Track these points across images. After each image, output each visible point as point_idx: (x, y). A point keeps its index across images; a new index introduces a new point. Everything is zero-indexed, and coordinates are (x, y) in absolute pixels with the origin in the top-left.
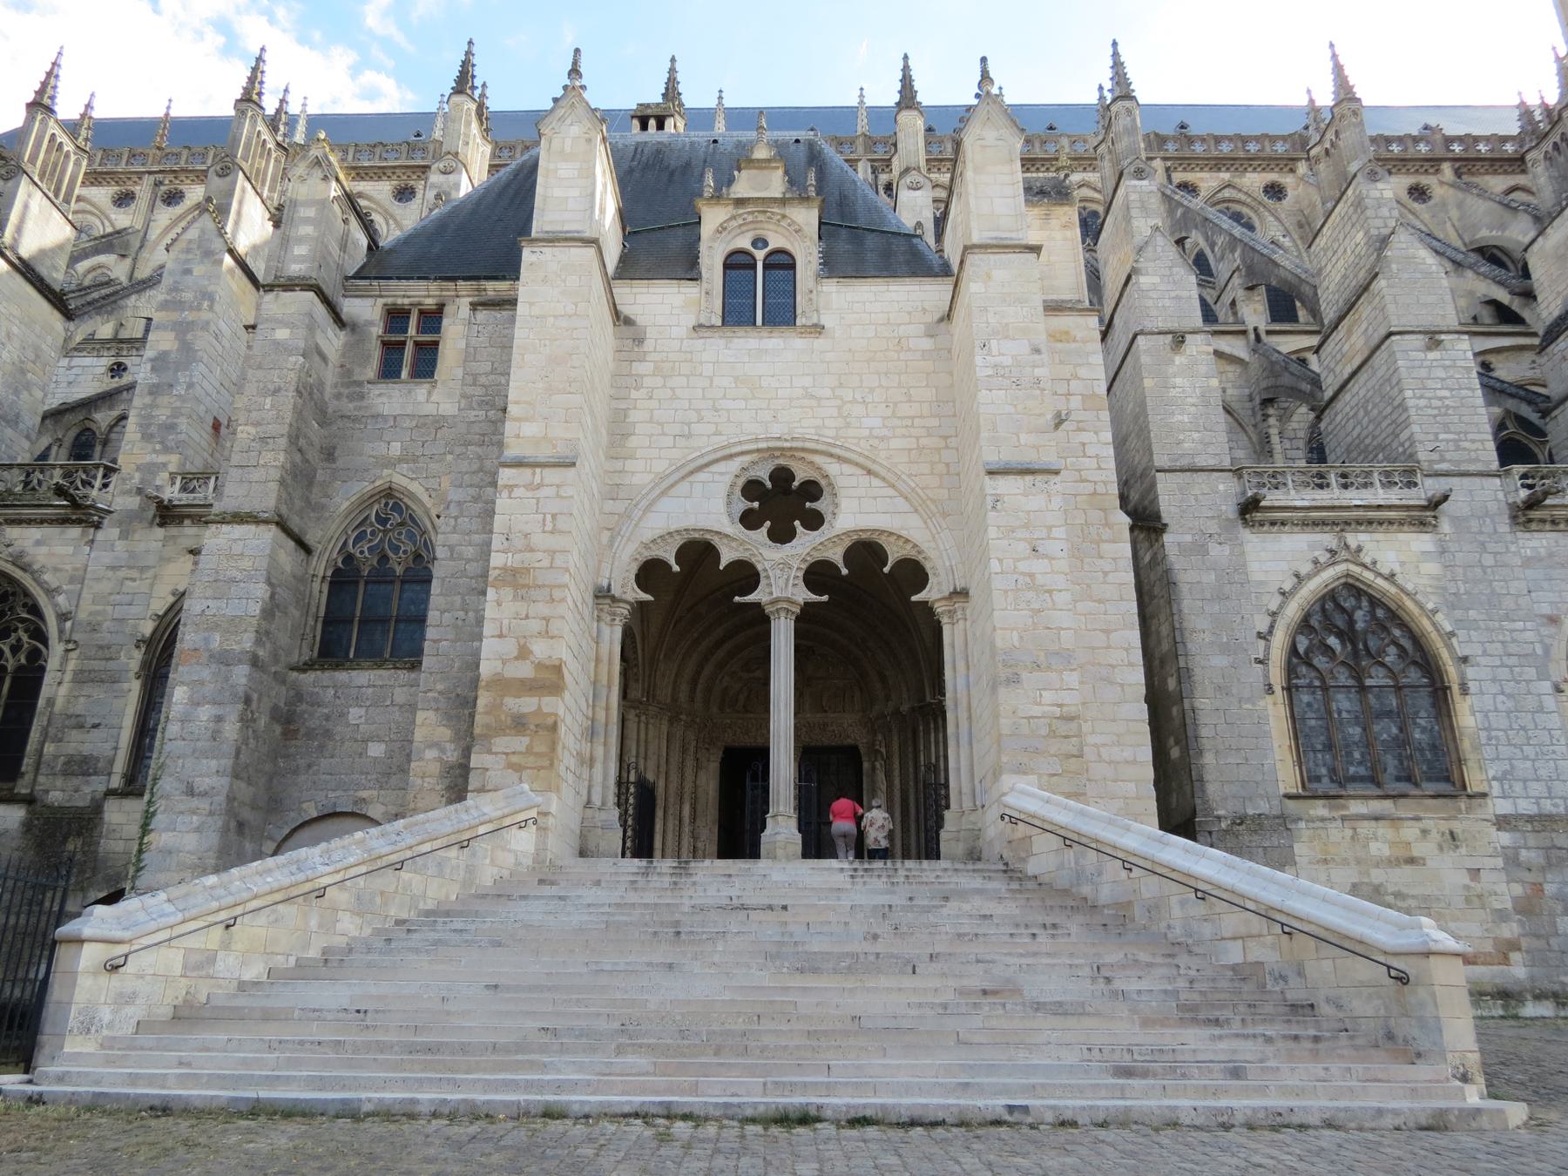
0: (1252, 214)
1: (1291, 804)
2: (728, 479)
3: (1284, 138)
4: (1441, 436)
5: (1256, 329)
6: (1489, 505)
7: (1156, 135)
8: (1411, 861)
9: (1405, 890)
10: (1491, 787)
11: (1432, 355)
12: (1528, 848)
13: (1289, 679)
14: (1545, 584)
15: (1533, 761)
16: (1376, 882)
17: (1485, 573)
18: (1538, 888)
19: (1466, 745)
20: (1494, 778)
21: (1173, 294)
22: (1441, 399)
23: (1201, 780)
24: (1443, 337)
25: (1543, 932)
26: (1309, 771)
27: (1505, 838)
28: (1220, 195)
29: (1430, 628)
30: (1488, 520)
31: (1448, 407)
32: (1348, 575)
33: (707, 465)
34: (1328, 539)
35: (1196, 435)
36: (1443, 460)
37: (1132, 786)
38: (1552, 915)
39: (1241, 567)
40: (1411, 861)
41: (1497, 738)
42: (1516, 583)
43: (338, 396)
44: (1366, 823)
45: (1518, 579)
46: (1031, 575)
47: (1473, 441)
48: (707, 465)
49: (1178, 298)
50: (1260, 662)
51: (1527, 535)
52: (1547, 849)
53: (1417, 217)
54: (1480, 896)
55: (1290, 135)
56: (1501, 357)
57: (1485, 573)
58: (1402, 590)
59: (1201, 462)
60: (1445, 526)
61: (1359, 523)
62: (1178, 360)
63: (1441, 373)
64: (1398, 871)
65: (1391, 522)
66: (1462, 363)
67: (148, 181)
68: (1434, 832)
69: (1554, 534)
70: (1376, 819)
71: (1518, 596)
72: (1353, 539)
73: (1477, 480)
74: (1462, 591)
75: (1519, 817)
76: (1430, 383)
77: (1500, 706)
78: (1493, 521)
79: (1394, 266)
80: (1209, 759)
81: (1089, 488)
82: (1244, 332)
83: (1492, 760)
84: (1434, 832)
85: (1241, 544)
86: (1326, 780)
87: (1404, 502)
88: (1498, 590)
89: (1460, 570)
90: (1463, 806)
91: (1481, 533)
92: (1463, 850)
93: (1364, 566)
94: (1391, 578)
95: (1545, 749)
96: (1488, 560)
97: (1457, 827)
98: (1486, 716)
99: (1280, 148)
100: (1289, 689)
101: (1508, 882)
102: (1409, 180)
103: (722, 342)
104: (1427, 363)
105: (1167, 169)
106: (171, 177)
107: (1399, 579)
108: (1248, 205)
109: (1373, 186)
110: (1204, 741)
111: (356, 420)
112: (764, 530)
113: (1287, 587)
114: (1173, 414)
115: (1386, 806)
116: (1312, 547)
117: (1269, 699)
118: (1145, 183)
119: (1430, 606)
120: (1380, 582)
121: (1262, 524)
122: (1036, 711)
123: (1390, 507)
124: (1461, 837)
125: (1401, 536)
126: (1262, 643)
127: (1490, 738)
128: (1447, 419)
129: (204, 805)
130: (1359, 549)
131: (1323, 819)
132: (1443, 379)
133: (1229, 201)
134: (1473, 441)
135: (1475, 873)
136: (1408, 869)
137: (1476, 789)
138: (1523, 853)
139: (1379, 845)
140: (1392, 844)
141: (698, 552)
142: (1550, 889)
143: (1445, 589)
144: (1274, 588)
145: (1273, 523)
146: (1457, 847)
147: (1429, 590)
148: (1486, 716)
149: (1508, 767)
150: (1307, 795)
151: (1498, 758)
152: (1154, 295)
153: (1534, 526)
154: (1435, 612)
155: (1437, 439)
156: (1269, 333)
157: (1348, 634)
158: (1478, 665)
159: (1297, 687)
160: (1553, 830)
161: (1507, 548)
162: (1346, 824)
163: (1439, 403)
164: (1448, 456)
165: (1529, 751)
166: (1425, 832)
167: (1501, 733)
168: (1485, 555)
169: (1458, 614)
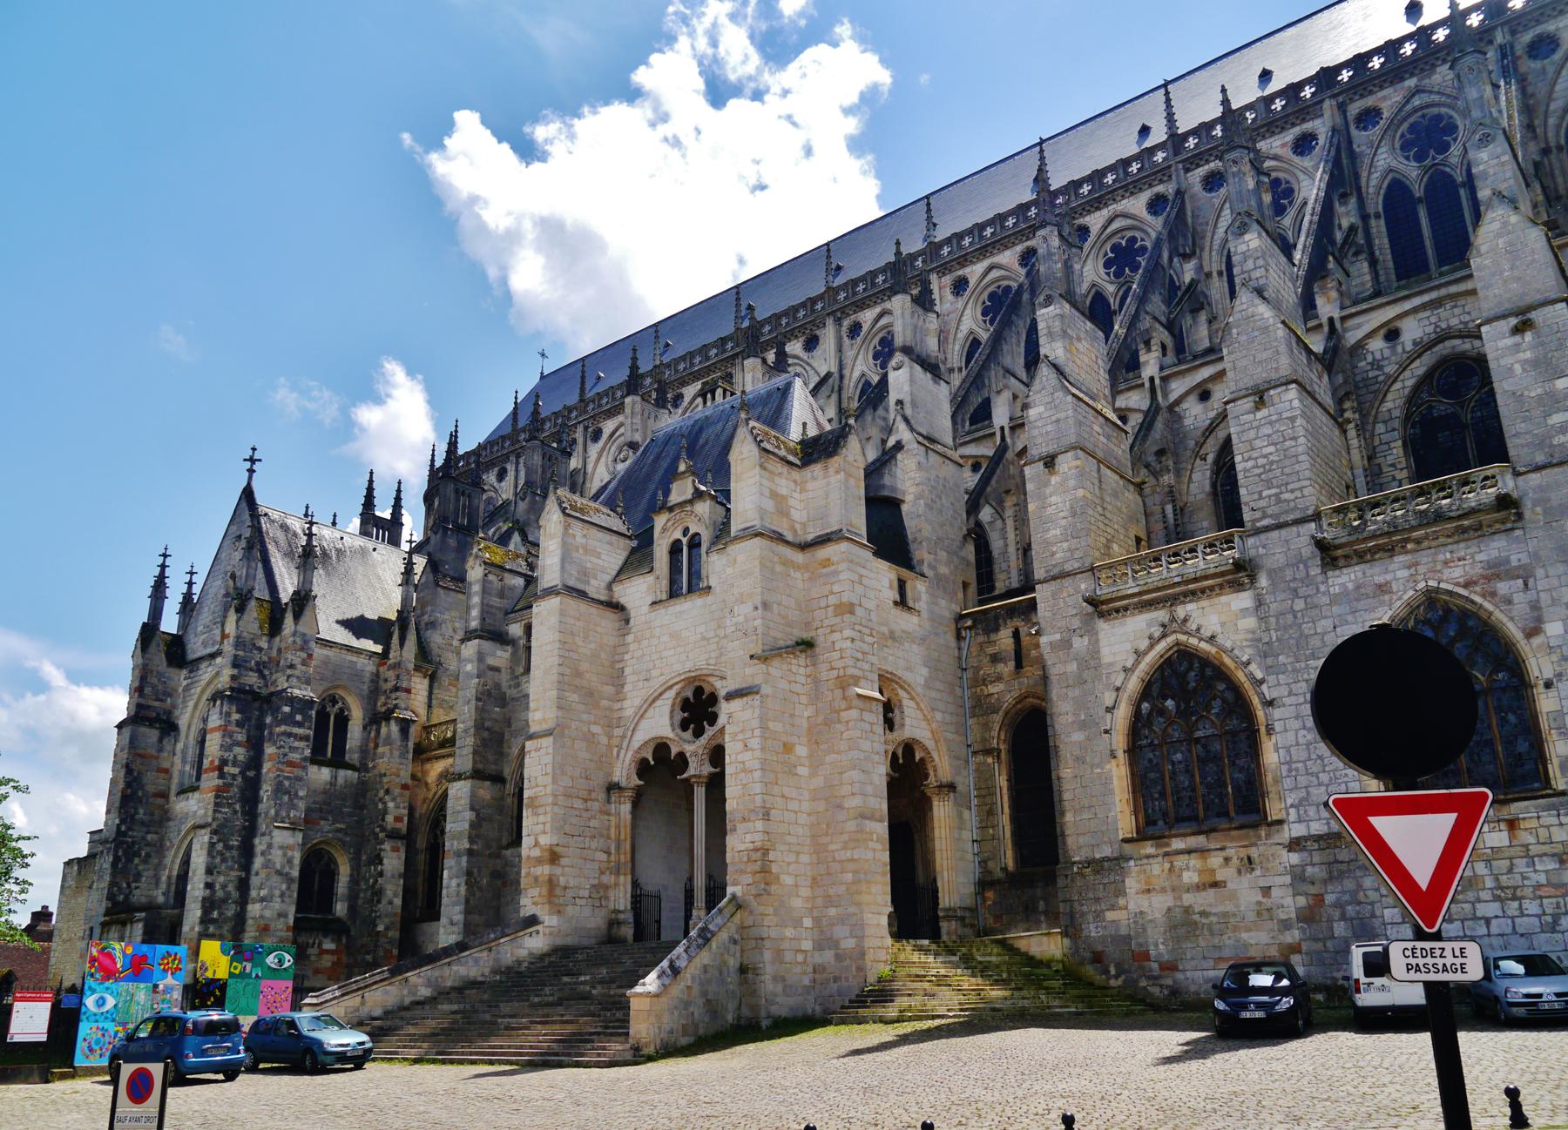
1: (1126, 846)
2: (670, 702)
4: (1264, 494)
5: (1331, 320)
6: (1303, 550)
8: (1215, 885)
9: (1208, 909)
10: (1288, 814)
11: (1259, 415)
12: (1313, 865)
13: (1134, 742)
14: (1350, 618)
15: (1327, 786)
16: (1186, 904)
17: (1295, 617)
18: (1319, 899)
19: (1269, 779)
20: (1292, 806)
21: (1054, 418)
22: (1265, 456)
23: (1063, 834)
24: (1272, 392)
25: (1321, 936)
26: (1147, 816)
27: (1295, 858)
28: (1409, 107)
29: (1243, 678)
30: (1301, 566)
31: (1272, 463)
32: (1178, 643)
33: (660, 695)
34: (1161, 615)
35: (1065, 545)
36: (1264, 516)
37: (850, 875)
38: (1330, 920)
39: (1095, 652)
40: (1215, 885)
41: (1297, 770)
42: (1323, 622)
43: (510, 687)
44: (1181, 857)
45: (1326, 617)
46: (743, 763)
47: (1292, 491)
48: (660, 695)
49: (1058, 421)
50: (1106, 732)
51: (1337, 572)
52: (1330, 864)
54: (1269, 910)
57: (1295, 617)
58: (1222, 649)
59: (1068, 567)
60: (1263, 581)
61: (1185, 595)
62: (1054, 480)
63: (1267, 430)
64: (1203, 894)
65: (1212, 588)
66: (1285, 415)
67: (580, 429)
68: (1235, 858)
69: (1363, 566)
70: (1189, 852)
71: (1324, 634)
72: (1181, 611)
73: (1294, 529)
74: (1274, 639)
75: (1306, 838)
76: (1258, 443)
77: (1301, 740)
78: (1306, 567)
79: (1234, 331)
80: (1069, 817)
81: (835, 673)
82: (1320, 326)
83: (1291, 790)
84: (1235, 858)
85: (1097, 634)
86: (1160, 823)
87: (1218, 570)
88: (1306, 632)
89: (1273, 620)
90: (1263, 833)
91: (1295, 579)
92: (1258, 872)
93: (1188, 634)
94: (1212, 639)
95: (1338, 773)
96: (1299, 605)
97: (1254, 853)
98: (1288, 751)
100: (1133, 751)
101: (1294, 896)
103: (663, 611)
104: (1255, 424)
105: (1342, 108)
106: (591, 421)
107: (1220, 639)
108: (1444, 105)
109: (1241, 240)
110: (1066, 804)
111: (517, 700)
112: (690, 731)
113: (1129, 664)
114: (1049, 530)
115: (1200, 841)
116: (1149, 625)
117: (1114, 762)
118: (1051, 308)
119: (1245, 659)
120: (1203, 645)
121: (1109, 613)
122: (742, 847)
123: (1206, 578)
124: (1257, 861)
125: (1224, 599)
126: (1109, 715)
127: (1290, 770)
128: (1271, 475)
129: (455, 929)
130: (1185, 620)
131: (1148, 857)
132: (1269, 436)
133: (1422, 108)
134: (1292, 491)
135: (1266, 891)
136: (1212, 891)
137: (1275, 818)
138: (1309, 869)
139: (1190, 874)
140: (1200, 872)
141: (661, 748)
142: (1330, 898)
143: (1260, 640)
144: (1119, 667)
145: (1117, 611)
146: (1253, 869)
147: (1245, 644)
148: (1288, 751)
149: (1304, 794)
150: (1141, 836)
151: (1296, 788)
152: (1039, 424)
153: (1342, 562)
154: (1248, 663)
155: (1261, 498)
156: (1343, 319)
157: (1182, 695)
158: (1284, 705)
159: (1141, 747)
160: (1336, 847)
161: (1318, 589)
162: (1166, 858)
163: (1264, 461)
164: (1269, 511)
165: (1324, 777)
166: (1227, 860)
167: (1300, 765)
168: (1296, 601)
169: (1269, 661)
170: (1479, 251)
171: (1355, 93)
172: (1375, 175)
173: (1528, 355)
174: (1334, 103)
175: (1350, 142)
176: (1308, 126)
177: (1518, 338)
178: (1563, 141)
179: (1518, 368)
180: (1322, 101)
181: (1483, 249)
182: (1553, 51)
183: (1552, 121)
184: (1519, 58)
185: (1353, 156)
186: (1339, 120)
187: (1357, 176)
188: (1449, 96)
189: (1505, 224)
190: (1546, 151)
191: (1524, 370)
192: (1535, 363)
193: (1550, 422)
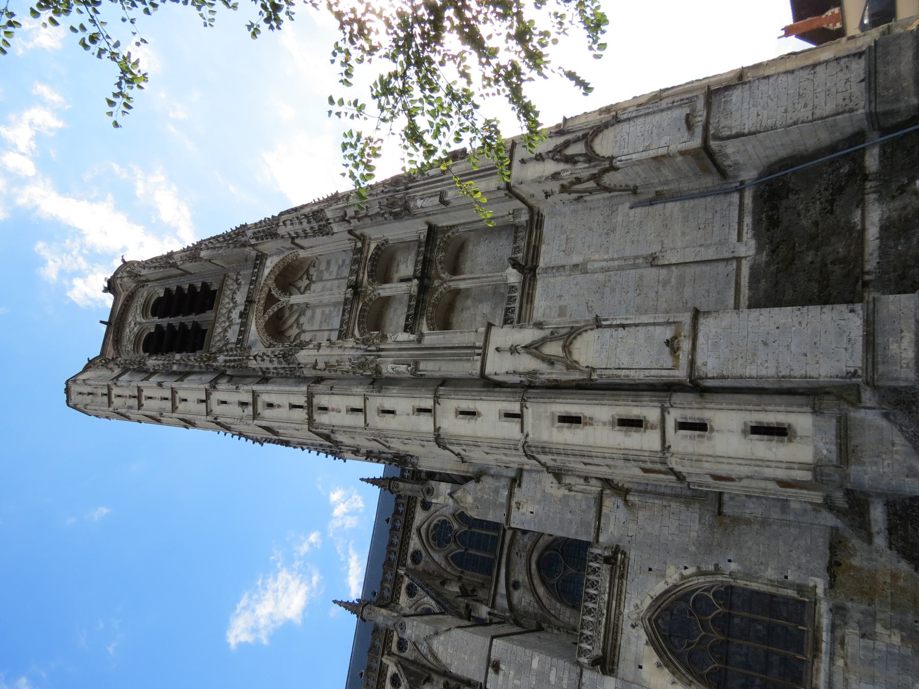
0: (422, 607)
3: (385, 573)
7: (369, 651)
53: (438, 510)
55: (384, 568)
56: (512, 574)
99: (389, 577)
102: (419, 509)
105: (390, 654)
170: (448, 664)
171: (388, 644)
172: (429, 657)
173: (512, 673)
174: (385, 656)
175: (407, 660)
176: (389, 674)
177: (501, 673)
178: (460, 569)
179: (517, 682)
180: (382, 662)
181: (449, 661)
182: (421, 554)
183: (449, 569)
184: (415, 569)
185: (414, 662)
186: (394, 659)
187: (424, 666)
188: (414, 604)
189: (443, 644)
190: (460, 578)
191: (519, 679)
192: (518, 672)
193: (553, 683)
